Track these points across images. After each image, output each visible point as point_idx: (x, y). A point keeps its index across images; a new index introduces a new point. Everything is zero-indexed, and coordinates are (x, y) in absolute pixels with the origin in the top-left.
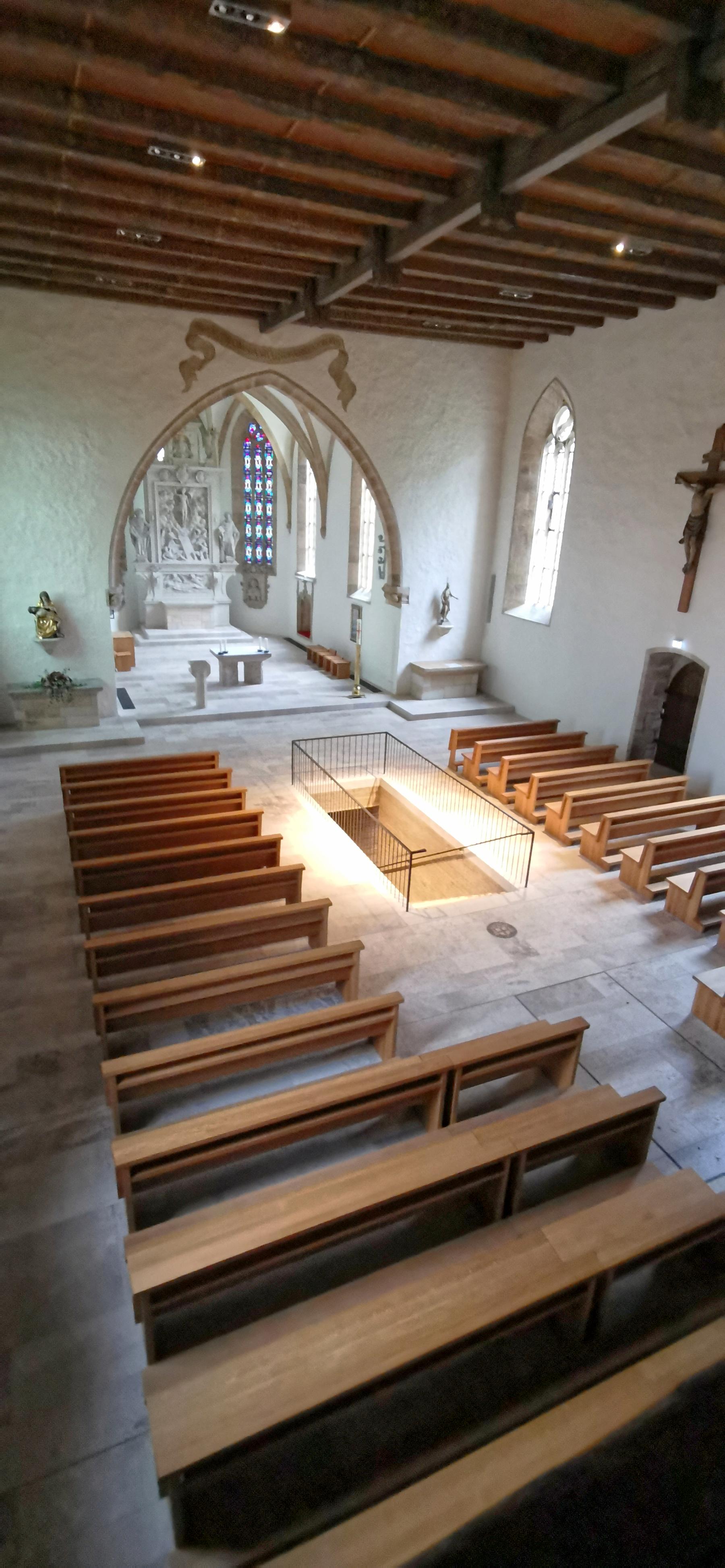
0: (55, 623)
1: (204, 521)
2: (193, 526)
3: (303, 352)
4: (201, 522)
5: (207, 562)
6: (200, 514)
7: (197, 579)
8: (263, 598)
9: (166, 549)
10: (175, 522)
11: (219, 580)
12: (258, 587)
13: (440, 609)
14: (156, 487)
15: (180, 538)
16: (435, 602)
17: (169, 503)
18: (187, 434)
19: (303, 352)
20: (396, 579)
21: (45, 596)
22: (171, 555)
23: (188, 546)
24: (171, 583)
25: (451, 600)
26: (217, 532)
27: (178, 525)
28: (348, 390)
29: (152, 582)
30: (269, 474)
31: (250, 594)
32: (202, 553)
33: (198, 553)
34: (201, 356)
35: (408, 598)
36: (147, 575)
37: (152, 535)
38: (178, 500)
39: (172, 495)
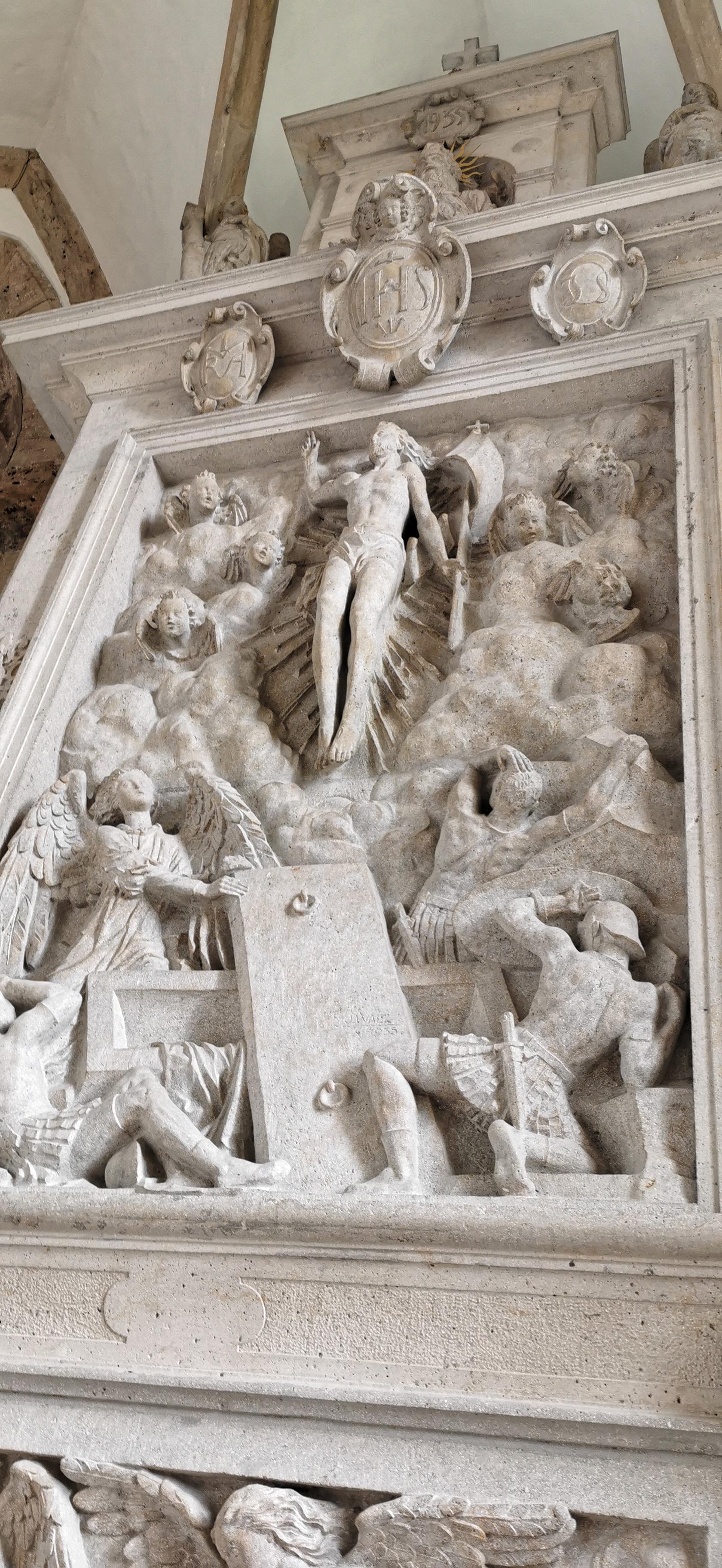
2: (451, 733)
6: (557, 607)
15: (254, 888)
27: (264, 754)
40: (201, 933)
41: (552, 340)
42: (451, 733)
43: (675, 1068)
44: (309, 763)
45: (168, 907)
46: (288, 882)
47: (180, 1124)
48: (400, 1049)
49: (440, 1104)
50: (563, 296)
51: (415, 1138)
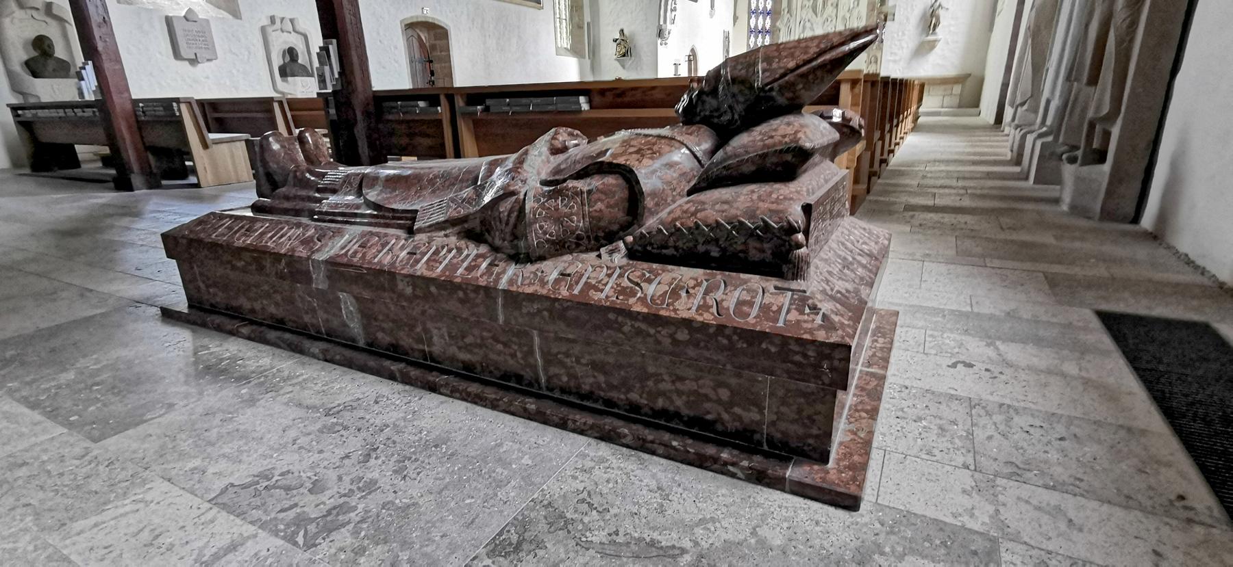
2: (825, 16)
13: (930, 21)
16: (924, 16)
25: (941, 12)
26: (844, 18)
37: (792, 25)
42: (825, 16)
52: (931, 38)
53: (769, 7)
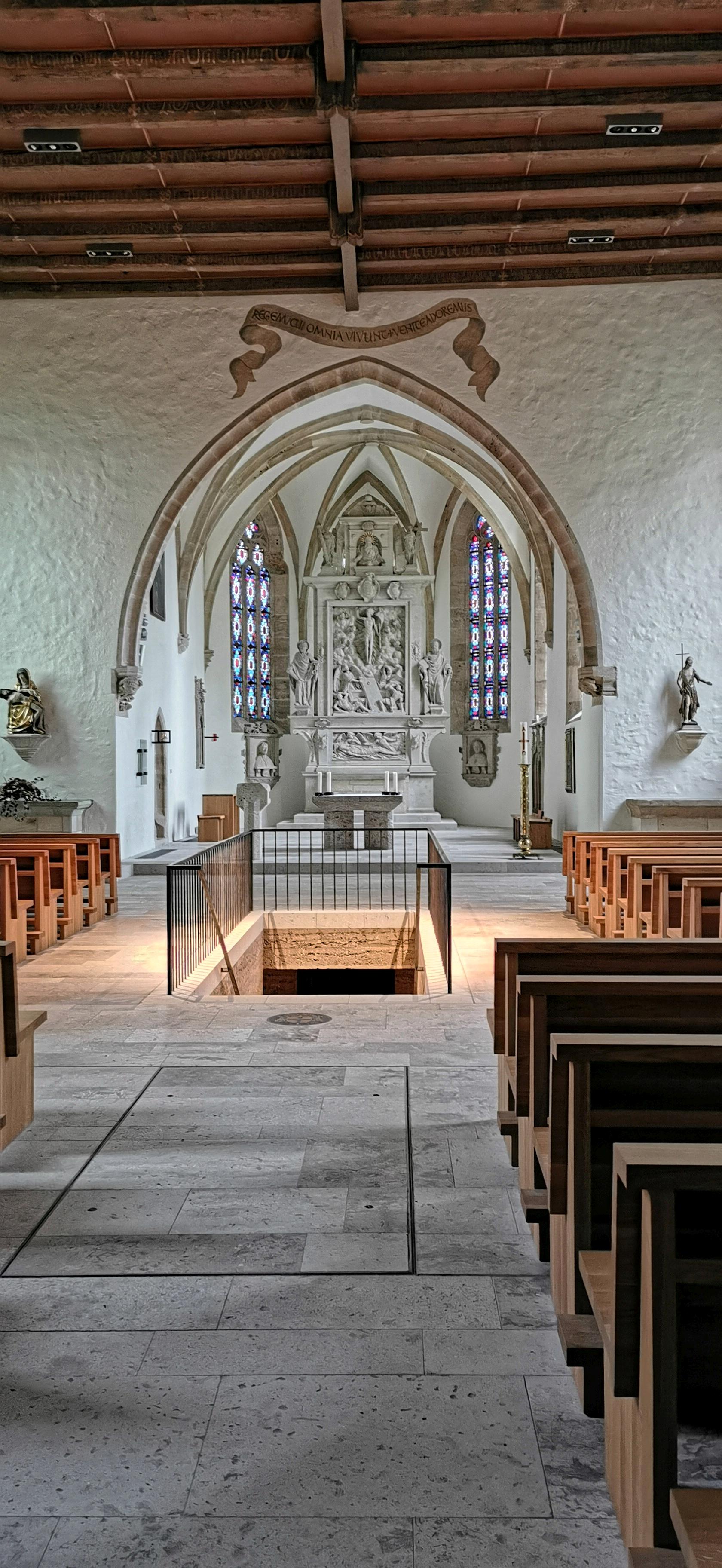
0: (32, 711)
1: (399, 654)
3: (414, 327)
4: (393, 656)
5: (403, 713)
6: (392, 645)
7: (384, 740)
8: (490, 770)
9: (340, 695)
10: (356, 656)
11: (419, 740)
12: (483, 753)
14: (328, 608)
16: (667, 689)
17: (347, 631)
18: (377, 533)
19: (414, 327)
20: (591, 655)
21: (24, 675)
22: (347, 705)
23: (374, 693)
24: (344, 746)
25: (697, 686)
27: (360, 662)
28: (486, 372)
29: (316, 743)
30: (506, 581)
31: (471, 764)
32: (393, 701)
33: (387, 700)
34: (260, 349)
35: (615, 686)
36: (309, 733)
37: (319, 676)
38: (361, 625)
39: (353, 618)
40: (358, 685)
41: (390, 599)
43: (404, 701)
44: (366, 663)
45: (353, 682)
46: (367, 680)
47: (363, 707)
48: (382, 701)
49: (385, 704)
50: (392, 592)
51: (384, 707)
52: (687, 730)
53: (265, 637)
